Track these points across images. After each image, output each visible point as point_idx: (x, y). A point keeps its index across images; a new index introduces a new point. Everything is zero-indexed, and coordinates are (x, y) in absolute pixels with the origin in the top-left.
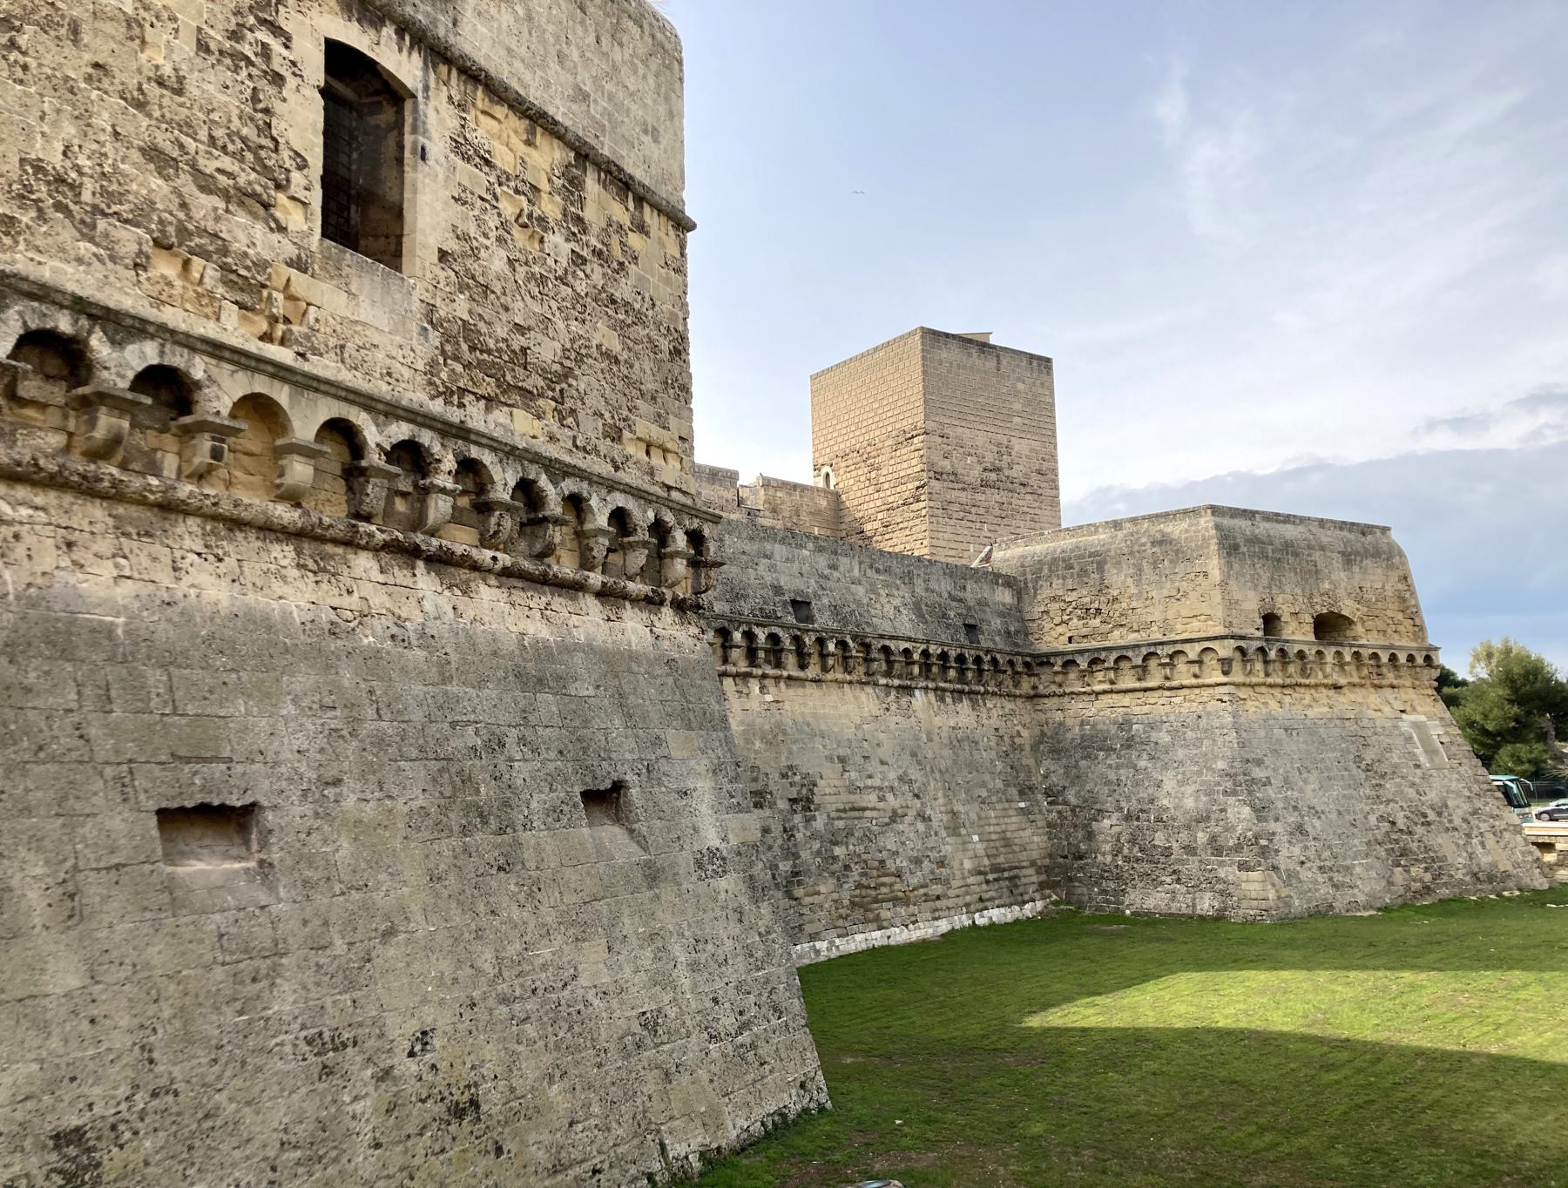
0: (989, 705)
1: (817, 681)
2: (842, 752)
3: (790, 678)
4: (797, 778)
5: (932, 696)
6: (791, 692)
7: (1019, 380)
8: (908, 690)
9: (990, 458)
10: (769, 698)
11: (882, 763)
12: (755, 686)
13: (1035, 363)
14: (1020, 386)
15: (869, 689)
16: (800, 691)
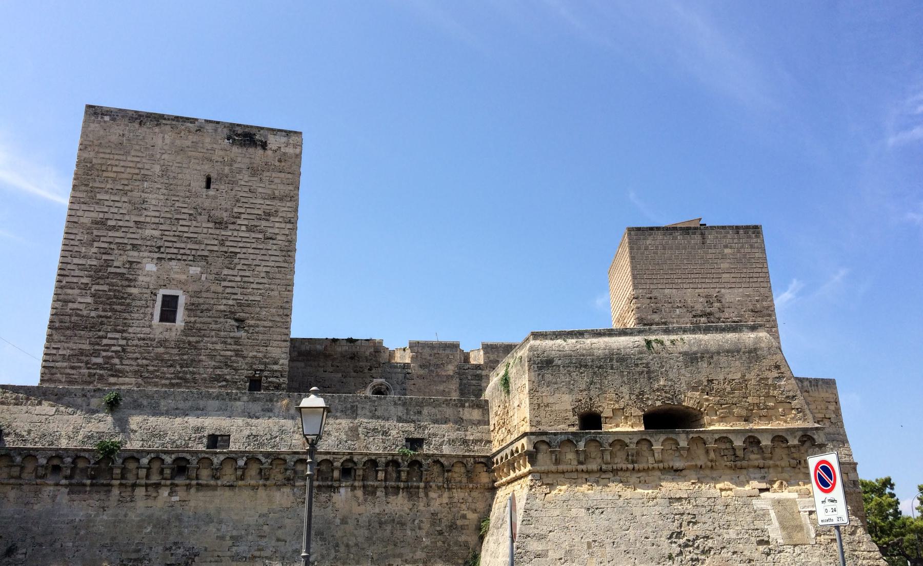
0: (432, 495)
1: (231, 486)
2: (235, 533)
3: (198, 484)
4: (181, 551)
5: (359, 493)
6: (200, 494)
7: (726, 247)
8: (334, 489)
9: (699, 307)
10: (175, 499)
11: (278, 540)
12: (165, 493)
13: (741, 232)
14: (727, 251)
15: (287, 490)
16: (210, 493)
